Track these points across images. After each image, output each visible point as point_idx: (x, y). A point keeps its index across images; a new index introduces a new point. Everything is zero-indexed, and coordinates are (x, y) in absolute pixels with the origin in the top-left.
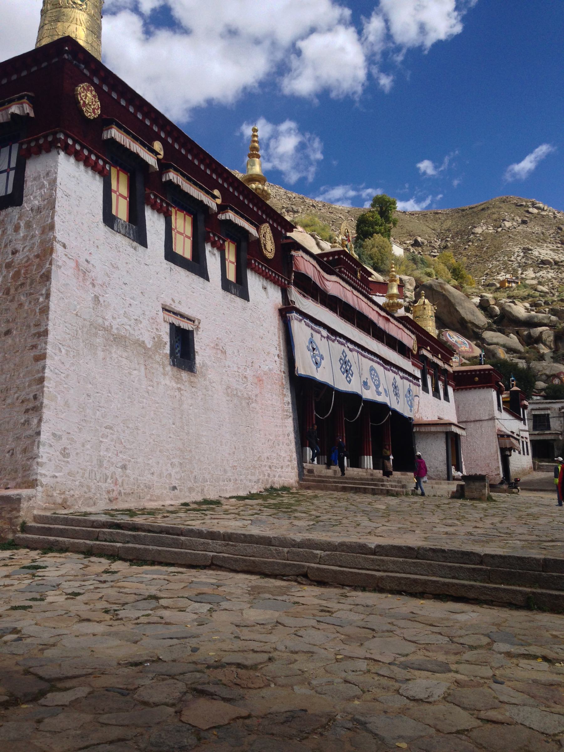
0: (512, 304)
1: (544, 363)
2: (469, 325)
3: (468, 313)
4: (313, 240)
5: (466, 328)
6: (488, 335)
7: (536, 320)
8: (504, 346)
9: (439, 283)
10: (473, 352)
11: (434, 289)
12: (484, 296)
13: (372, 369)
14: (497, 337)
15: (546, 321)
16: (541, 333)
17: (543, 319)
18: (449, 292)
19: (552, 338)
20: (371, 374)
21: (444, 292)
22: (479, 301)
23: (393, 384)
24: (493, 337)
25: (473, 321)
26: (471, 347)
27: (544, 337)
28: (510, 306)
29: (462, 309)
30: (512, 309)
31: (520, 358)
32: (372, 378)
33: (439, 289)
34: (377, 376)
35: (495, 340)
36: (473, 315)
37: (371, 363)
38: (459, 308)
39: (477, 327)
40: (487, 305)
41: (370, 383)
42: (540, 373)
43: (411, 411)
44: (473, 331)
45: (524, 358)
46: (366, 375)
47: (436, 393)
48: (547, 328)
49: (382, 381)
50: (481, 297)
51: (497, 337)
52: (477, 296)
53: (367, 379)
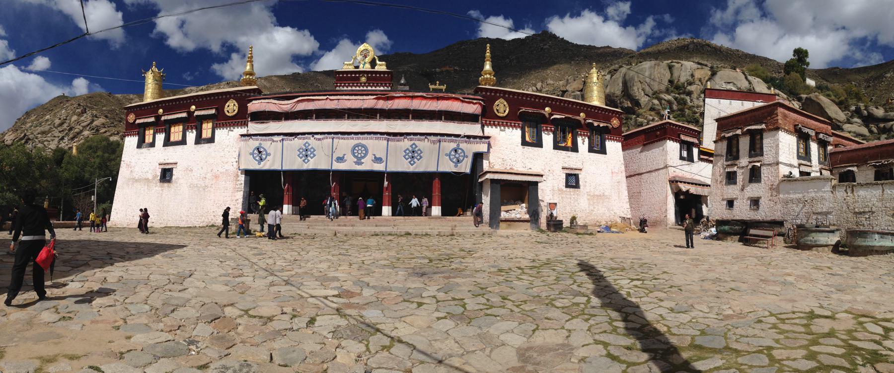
33: (815, 99)
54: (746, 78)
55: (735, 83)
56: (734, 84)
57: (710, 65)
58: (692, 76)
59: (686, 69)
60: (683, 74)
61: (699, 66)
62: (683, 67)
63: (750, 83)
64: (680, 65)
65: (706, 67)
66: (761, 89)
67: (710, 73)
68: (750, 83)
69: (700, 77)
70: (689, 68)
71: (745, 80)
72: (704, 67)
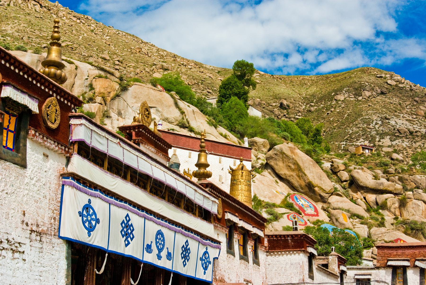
0: (360, 171)
1: (383, 229)
2: (316, 189)
3: (316, 177)
4: (171, 100)
5: (314, 192)
6: (334, 200)
7: (381, 187)
8: (348, 211)
9: (289, 147)
10: (317, 215)
11: (284, 153)
12: (335, 161)
13: (159, 233)
14: (342, 202)
15: (391, 189)
16: (386, 199)
17: (389, 187)
18: (299, 157)
19: (397, 205)
20: (157, 238)
21: (294, 157)
22: (330, 166)
23: (183, 246)
24: (338, 202)
25: (320, 185)
26: (316, 210)
27: (389, 204)
28: (358, 172)
29: (310, 173)
30: (360, 175)
31: (362, 223)
32: (157, 243)
34: (164, 240)
35: (340, 205)
36: (321, 180)
37: (159, 228)
38: (307, 172)
39: (324, 190)
40: (338, 171)
41: (154, 247)
42: (379, 239)
43: (205, 273)
44: (321, 196)
45: (366, 224)
46: (151, 238)
47: (244, 256)
48: (392, 195)
49: (169, 244)
50: (332, 162)
51: (342, 202)
52: (328, 161)
53: (152, 242)
54: (176, 104)
55: (160, 109)
56: (158, 111)
57: (117, 74)
58: (91, 87)
59: (83, 74)
60: (78, 82)
61: (103, 73)
62: (79, 70)
63: (183, 113)
64: (73, 66)
65: (112, 77)
66: (199, 124)
67: (117, 87)
68: (183, 113)
69: (102, 91)
70: (86, 74)
71: (174, 107)
72: (108, 75)
